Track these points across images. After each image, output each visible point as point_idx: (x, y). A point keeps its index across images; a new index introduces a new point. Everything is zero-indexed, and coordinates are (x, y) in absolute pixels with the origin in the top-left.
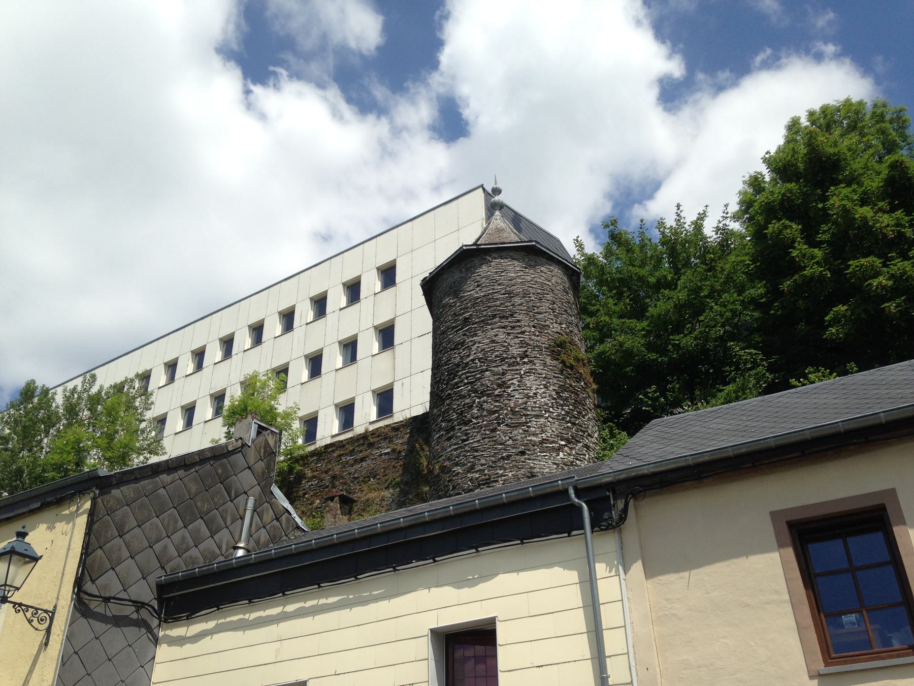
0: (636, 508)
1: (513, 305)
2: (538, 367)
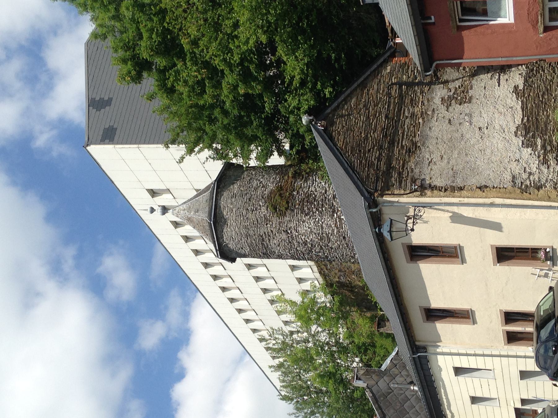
0: (419, 341)
1: (255, 235)
2: (292, 225)
